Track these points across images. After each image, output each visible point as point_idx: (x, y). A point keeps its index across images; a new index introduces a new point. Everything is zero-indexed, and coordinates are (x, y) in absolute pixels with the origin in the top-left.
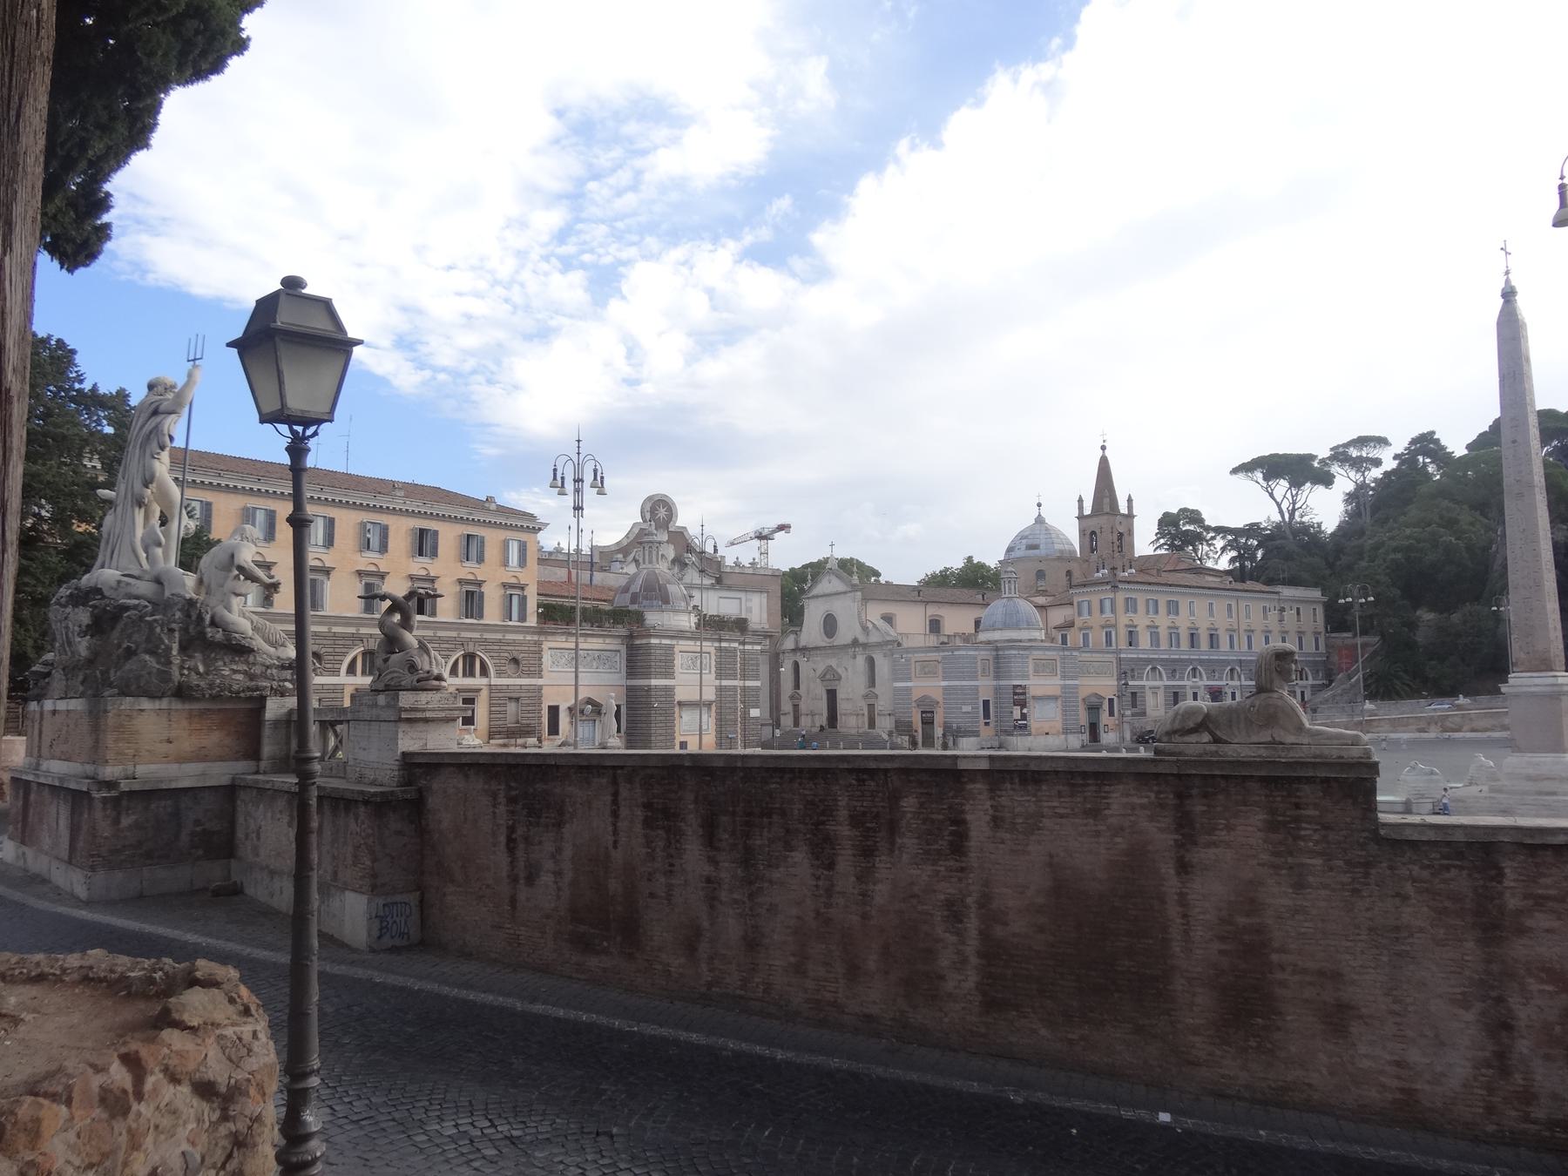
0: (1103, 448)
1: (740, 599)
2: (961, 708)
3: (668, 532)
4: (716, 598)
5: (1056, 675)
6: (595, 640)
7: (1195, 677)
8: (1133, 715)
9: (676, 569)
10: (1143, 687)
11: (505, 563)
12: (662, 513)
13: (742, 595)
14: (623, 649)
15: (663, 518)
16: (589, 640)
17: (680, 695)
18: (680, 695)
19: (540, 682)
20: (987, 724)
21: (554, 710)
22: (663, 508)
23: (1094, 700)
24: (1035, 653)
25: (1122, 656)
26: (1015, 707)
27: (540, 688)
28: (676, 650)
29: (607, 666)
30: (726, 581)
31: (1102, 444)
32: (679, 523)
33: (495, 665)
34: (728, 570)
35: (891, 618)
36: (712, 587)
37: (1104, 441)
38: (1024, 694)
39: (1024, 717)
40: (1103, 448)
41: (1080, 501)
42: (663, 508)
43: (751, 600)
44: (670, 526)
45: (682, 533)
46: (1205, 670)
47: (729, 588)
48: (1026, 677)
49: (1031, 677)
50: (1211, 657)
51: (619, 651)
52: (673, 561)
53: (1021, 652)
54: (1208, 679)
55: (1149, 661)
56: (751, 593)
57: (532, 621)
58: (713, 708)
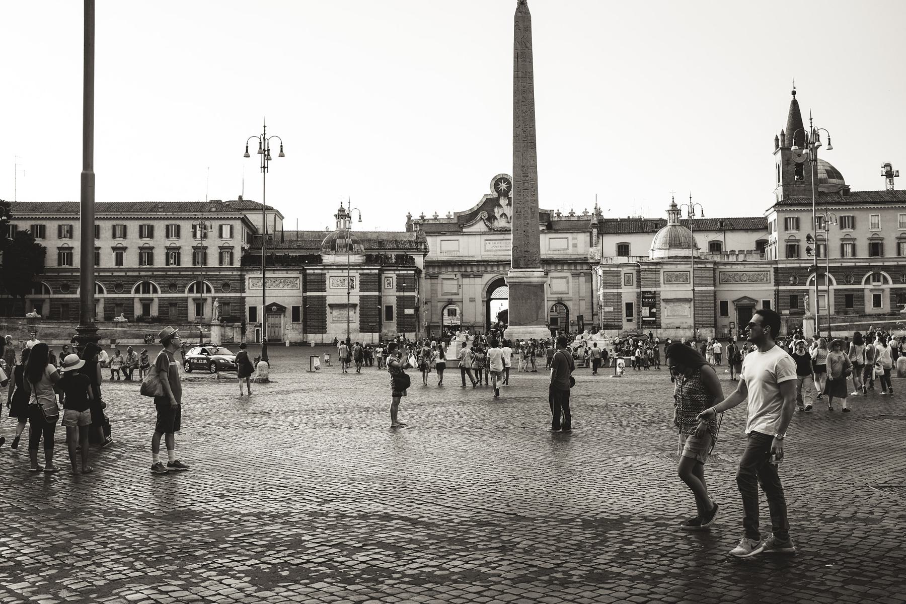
0: (794, 93)
1: (566, 238)
2: (614, 309)
4: (547, 239)
5: (690, 283)
6: (280, 272)
7: (879, 281)
8: (791, 314)
10: (863, 290)
11: (221, 236)
12: (503, 186)
13: (569, 236)
14: (301, 276)
16: (276, 272)
17: (330, 300)
18: (330, 300)
19: (243, 295)
20: (628, 320)
21: (253, 310)
23: (746, 301)
24: (665, 267)
25: (780, 266)
26: (644, 308)
27: (244, 298)
28: (327, 276)
29: (290, 286)
30: (554, 227)
31: (793, 90)
33: (214, 287)
35: (628, 246)
37: (794, 88)
38: (654, 298)
39: (652, 315)
40: (794, 93)
41: (777, 139)
43: (576, 239)
46: (890, 275)
47: (556, 231)
48: (658, 285)
49: (662, 285)
50: (900, 263)
51: (298, 278)
53: (651, 267)
54: (894, 283)
55: (870, 268)
56: (575, 234)
57: (237, 264)
58: (358, 308)
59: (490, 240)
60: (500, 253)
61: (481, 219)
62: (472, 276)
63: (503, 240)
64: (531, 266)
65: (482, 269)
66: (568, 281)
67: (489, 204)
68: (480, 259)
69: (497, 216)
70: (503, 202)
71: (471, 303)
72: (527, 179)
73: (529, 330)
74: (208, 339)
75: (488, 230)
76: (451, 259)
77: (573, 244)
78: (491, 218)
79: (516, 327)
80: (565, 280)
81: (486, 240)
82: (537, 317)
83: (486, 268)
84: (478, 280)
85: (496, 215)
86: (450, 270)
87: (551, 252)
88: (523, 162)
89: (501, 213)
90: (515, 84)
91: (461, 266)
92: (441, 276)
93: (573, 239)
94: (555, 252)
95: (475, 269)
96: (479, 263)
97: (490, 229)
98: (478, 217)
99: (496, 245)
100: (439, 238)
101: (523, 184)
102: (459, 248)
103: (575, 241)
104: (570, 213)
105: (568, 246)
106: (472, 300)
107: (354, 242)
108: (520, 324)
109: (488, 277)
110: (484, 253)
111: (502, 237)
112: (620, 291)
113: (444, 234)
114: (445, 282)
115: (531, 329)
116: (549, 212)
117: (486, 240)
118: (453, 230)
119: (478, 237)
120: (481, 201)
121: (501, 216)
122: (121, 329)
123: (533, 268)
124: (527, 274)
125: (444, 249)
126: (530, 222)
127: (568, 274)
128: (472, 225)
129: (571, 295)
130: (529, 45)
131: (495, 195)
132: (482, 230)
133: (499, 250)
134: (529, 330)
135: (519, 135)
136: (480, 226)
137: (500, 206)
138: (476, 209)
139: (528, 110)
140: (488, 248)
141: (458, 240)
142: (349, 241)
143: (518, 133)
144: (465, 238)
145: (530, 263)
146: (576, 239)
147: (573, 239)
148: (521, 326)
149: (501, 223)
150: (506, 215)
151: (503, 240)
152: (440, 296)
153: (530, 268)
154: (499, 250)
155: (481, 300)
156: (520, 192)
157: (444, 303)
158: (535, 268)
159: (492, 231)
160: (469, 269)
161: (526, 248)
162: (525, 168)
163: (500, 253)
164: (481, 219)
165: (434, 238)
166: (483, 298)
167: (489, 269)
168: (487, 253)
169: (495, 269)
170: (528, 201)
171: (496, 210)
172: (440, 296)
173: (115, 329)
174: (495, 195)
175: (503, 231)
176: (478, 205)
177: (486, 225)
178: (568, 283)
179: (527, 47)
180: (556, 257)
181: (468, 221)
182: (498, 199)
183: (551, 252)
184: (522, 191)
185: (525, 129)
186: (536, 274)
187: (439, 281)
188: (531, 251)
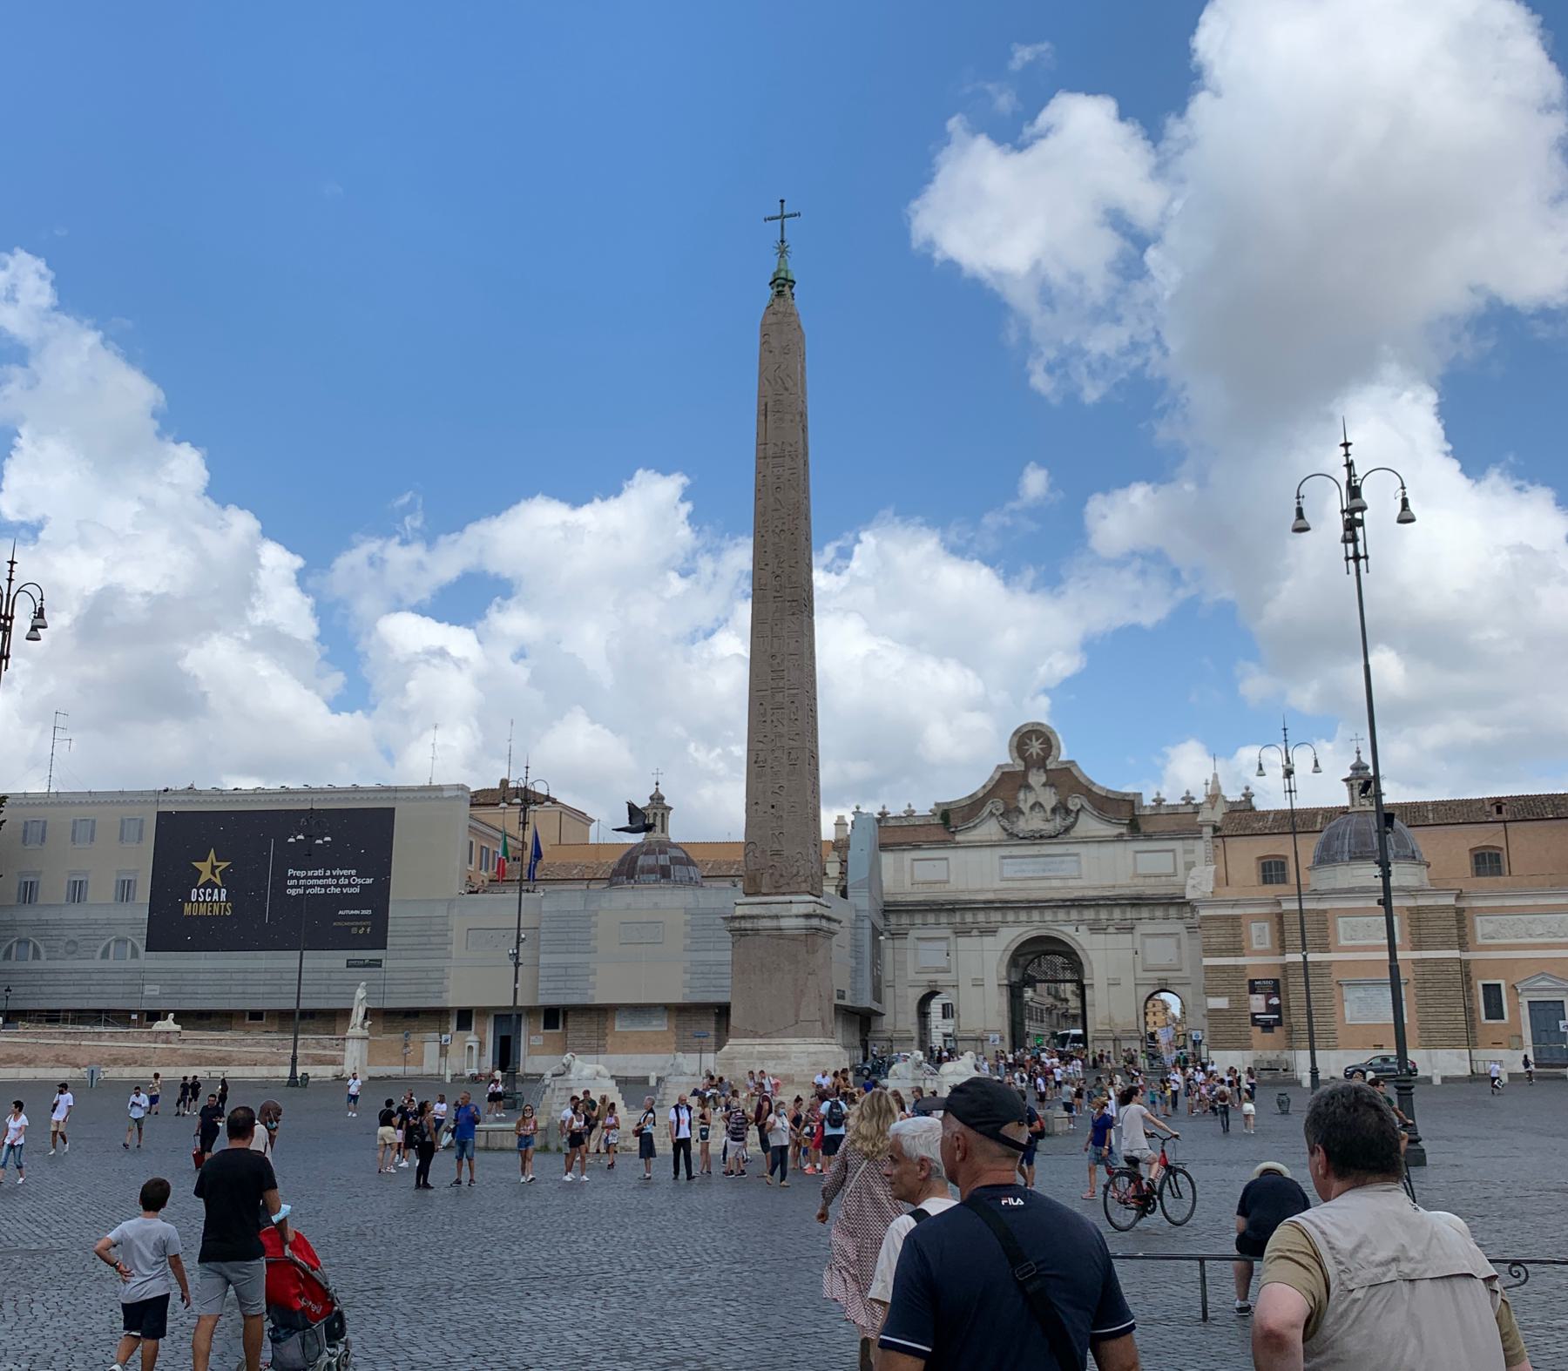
1: (1173, 851)
3: (1046, 771)
9: (1058, 819)
12: (1035, 747)
13: (1177, 845)
15: (1038, 754)
22: (1037, 740)
30: (1144, 828)
32: (1064, 757)
34: (1147, 812)
36: (1119, 838)
42: (1037, 740)
43: (1192, 852)
44: (1048, 762)
45: (1068, 769)
47: (1149, 837)
52: (1054, 810)
56: (1191, 842)
59: (1011, 857)
60: (1032, 884)
61: (992, 814)
62: (975, 932)
63: (1037, 856)
64: (781, 890)
65: (996, 917)
66: (1179, 941)
67: (1006, 785)
68: (990, 896)
69: (1025, 807)
70: (1036, 778)
71: (976, 988)
72: (781, 685)
73: (774, 1048)
74: (340, 1067)
75: (1005, 837)
76: (932, 899)
77: (1186, 863)
78: (1011, 812)
79: (747, 1041)
80: (1172, 941)
81: (1004, 857)
82: (797, 1015)
83: (1004, 916)
84: (988, 941)
85: (1021, 805)
86: (931, 918)
87: (1140, 881)
88: (772, 647)
89: (1031, 802)
90: (758, 472)
91: (953, 910)
92: (913, 933)
93: (1186, 852)
94: (1147, 880)
95: (981, 917)
96: (989, 906)
97: (1011, 835)
98: (986, 811)
99: (1024, 867)
100: (909, 856)
101: (773, 695)
102: (948, 876)
103: (1190, 858)
104: (1183, 799)
105: (1175, 869)
106: (978, 983)
107: (675, 861)
108: (756, 1035)
109: (1012, 934)
110: (998, 885)
111: (1034, 850)
112: (1241, 961)
113: (917, 847)
114: (922, 945)
115: (780, 1048)
116: (1131, 798)
117: (1004, 857)
118: (935, 838)
119: (988, 851)
120: (992, 777)
121: (1032, 808)
122: (164, 1046)
123: (791, 893)
124: (775, 910)
125: (918, 877)
126: (784, 783)
127: (1179, 927)
128: (975, 826)
129: (1186, 973)
130: (789, 384)
131: (1020, 766)
132: (994, 838)
133: (1031, 879)
134: (774, 1048)
135: (765, 585)
136: (990, 829)
137: (1028, 787)
138: (981, 795)
139: (785, 528)
140: (1006, 875)
141: (946, 859)
142: (663, 860)
143: (763, 581)
144: (961, 853)
145: (782, 881)
146: (1192, 852)
147: (1186, 852)
148: (758, 1041)
149: (1032, 822)
150: (1041, 806)
151: (1037, 856)
152: (911, 975)
153: (784, 894)
154: (1031, 879)
155: (996, 983)
156: (764, 715)
157: (921, 989)
158: (796, 893)
159: (1013, 837)
160: (969, 917)
161: (776, 847)
162: (777, 661)
163: (1032, 884)
164: (992, 814)
165: (899, 855)
166: (999, 979)
167: (1011, 917)
168: (1005, 885)
169: (1023, 916)
170: (782, 736)
171: (1021, 796)
172: (911, 975)
173: (153, 1045)
174: (1020, 766)
175: (1036, 838)
176: (984, 787)
177: (1005, 830)
178: (1179, 947)
179: (786, 389)
180: (1149, 892)
181: (966, 819)
182: (1025, 774)
183: (1140, 881)
184: (769, 712)
185: (779, 572)
186: (796, 909)
187: (910, 942)
188: (785, 853)
